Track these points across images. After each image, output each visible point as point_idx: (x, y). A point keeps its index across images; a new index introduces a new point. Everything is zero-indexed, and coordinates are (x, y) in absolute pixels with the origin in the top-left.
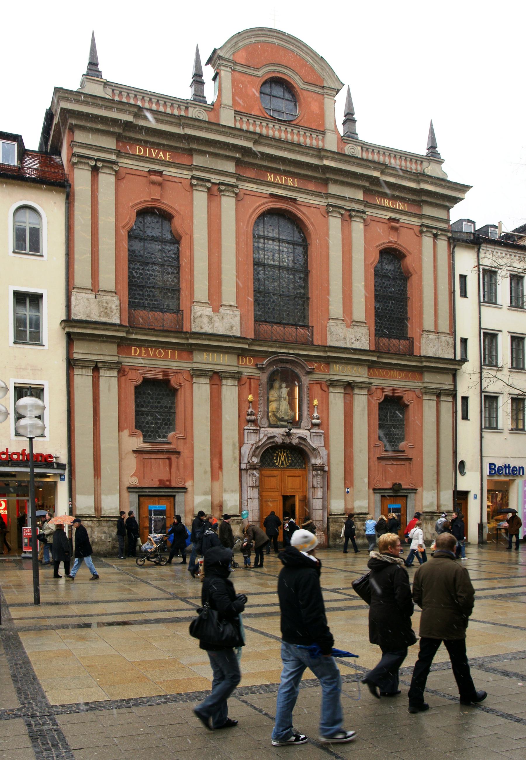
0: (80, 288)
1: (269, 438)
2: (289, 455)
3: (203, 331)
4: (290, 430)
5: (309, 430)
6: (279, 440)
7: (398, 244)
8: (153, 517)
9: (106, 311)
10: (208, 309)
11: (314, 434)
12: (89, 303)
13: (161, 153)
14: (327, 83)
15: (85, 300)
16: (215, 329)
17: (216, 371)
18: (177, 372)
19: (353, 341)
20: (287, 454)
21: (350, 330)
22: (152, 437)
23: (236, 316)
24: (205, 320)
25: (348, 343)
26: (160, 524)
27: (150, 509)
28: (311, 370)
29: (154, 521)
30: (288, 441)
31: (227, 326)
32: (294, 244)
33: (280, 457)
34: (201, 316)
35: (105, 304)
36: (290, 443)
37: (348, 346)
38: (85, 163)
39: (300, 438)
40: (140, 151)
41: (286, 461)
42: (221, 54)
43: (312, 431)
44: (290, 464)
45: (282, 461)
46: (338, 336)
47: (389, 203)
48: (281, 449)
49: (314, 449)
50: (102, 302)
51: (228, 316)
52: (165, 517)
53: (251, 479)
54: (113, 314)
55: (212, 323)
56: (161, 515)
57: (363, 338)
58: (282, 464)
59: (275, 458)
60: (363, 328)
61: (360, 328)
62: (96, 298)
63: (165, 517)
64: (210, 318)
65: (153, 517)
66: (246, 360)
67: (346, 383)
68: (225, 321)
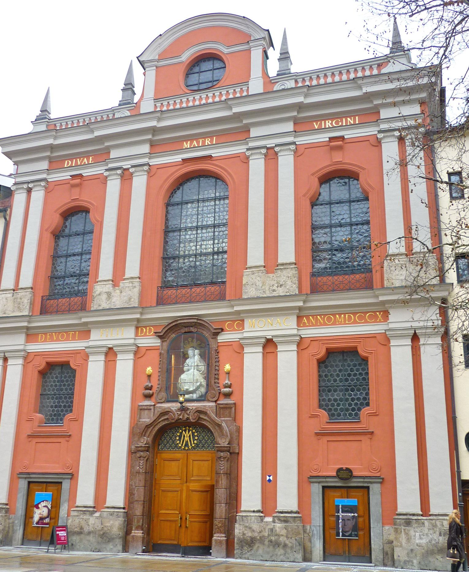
0: (4, 290)
2: (196, 434)
3: (101, 308)
6: (177, 415)
8: (341, 514)
10: (107, 286)
11: (221, 406)
12: (7, 301)
13: (85, 159)
14: (254, 37)
15: (4, 300)
18: (76, 353)
19: (275, 288)
20: (193, 433)
21: (271, 275)
22: (55, 421)
23: (135, 287)
24: (104, 297)
25: (267, 292)
26: (350, 524)
27: (336, 504)
28: (220, 331)
29: (342, 520)
31: (126, 299)
34: (99, 294)
35: (19, 300)
37: (268, 294)
41: (190, 441)
43: (218, 402)
44: (197, 445)
46: (254, 286)
47: (331, 124)
48: (189, 427)
52: (356, 515)
55: (110, 298)
56: (351, 513)
57: (289, 283)
58: (187, 445)
59: (177, 438)
60: (289, 270)
63: (356, 515)
64: (109, 294)
65: (341, 514)
67: (264, 340)
68: (124, 294)
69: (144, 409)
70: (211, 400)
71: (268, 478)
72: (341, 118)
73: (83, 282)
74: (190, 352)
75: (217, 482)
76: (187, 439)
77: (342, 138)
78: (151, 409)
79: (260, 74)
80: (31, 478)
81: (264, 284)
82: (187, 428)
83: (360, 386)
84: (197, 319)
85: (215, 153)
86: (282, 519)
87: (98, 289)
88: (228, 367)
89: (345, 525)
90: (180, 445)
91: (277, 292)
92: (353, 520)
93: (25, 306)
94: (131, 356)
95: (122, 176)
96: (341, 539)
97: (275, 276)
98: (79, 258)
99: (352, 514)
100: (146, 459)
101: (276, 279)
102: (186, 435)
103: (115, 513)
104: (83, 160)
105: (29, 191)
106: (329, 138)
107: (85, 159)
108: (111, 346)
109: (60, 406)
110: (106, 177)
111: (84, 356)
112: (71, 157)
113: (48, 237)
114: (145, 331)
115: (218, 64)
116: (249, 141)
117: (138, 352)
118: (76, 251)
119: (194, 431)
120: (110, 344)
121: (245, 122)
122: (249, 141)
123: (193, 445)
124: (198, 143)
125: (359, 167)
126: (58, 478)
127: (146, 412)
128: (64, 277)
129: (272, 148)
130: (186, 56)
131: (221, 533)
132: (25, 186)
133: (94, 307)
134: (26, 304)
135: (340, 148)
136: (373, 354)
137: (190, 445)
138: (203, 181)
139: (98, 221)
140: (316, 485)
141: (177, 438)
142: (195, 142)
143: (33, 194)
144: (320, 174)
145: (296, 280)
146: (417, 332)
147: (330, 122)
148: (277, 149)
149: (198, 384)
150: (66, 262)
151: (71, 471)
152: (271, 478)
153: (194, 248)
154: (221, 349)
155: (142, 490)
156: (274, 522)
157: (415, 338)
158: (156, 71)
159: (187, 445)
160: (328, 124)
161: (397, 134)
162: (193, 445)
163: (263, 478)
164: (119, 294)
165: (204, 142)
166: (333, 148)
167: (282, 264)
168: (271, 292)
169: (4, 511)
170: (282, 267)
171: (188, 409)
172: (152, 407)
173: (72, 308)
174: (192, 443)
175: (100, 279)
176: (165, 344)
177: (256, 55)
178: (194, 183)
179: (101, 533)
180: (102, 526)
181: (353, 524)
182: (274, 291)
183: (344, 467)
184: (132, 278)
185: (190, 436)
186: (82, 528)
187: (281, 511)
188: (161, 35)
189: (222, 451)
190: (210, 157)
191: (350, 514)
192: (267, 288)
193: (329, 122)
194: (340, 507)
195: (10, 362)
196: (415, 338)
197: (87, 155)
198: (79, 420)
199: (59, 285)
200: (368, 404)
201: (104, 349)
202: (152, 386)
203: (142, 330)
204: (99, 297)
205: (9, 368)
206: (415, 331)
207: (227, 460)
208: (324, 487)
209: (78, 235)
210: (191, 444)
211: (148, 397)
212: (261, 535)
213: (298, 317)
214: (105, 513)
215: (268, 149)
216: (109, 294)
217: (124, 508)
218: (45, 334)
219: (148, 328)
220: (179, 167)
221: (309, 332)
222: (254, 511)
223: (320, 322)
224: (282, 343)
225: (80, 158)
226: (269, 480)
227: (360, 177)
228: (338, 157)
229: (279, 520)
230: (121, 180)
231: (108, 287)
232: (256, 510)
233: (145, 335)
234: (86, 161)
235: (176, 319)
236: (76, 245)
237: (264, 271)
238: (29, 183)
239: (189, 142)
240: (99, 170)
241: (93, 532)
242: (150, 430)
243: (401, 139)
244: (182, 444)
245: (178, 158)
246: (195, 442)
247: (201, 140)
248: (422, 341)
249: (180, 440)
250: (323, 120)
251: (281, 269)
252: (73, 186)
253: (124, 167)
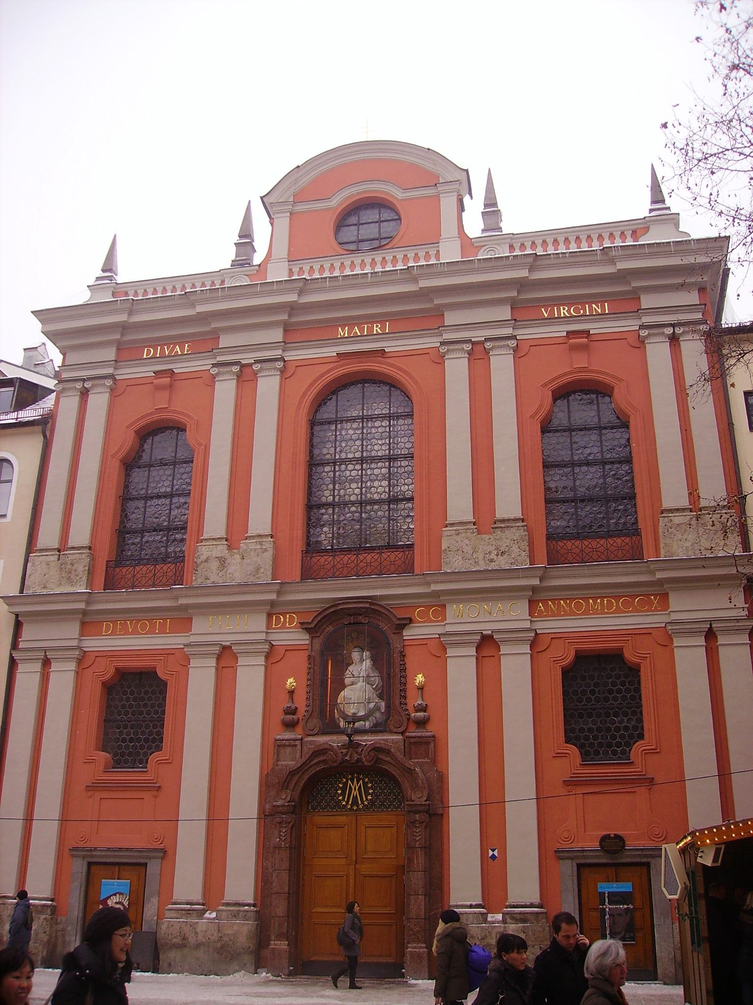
0: (43, 550)
3: (209, 583)
7: (591, 371)
9: (69, 575)
10: (220, 548)
11: (413, 740)
14: (444, 178)
15: (44, 566)
16: (228, 576)
17: (224, 644)
18: (167, 653)
19: (493, 556)
23: (266, 550)
24: (215, 565)
25: (482, 563)
32: (390, 417)
34: (206, 561)
35: (69, 567)
38: (71, 389)
40: (149, 352)
42: (271, 200)
43: (407, 734)
47: (569, 311)
48: (359, 774)
50: (66, 564)
51: (252, 553)
54: (78, 578)
57: (515, 549)
58: (355, 802)
59: (339, 792)
61: (507, 532)
62: (59, 560)
64: (222, 561)
66: (285, 618)
69: (285, 746)
70: (395, 730)
71: (491, 853)
72: (583, 304)
73: (175, 540)
74: (356, 655)
75: (410, 860)
76: (355, 792)
77: (586, 333)
78: (295, 746)
79: (455, 233)
80: (93, 856)
81: (475, 551)
83: (629, 708)
84: (371, 603)
85: (391, 346)
86: (518, 917)
87: (204, 551)
88: (420, 678)
89: (614, 923)
90: (344, 803)
91: (497, 563)
92: (627, 914)
93: (80, 576)
94: (261, 660)
95: (239, 376)
97: (492, 539)
98: (168, 501)
99: (625, 906)
100: (290, 825)
101: (494, 543)
102: (353, 788)
103: (241, 914)
104: (174, 347)
105: (84, 394)
106: (567, 332)
107: (177, 347)
108: (228, 644)
109: (139, 740)
110: (214, 377)
111: (183, 659)
112: (153, 343)
113: (115, 467)
114: (282, 620)
115: (386, 215)
116: (444, 330)
117: (271, 654)
118: (163, 490)
119: (366, 780)
120: (227, 640)
121: (437, 301)
122: (444, 330)
123: (366, 803)
124: (362, 330)
125: (614, 377)
126: (140, 857)
127: (289, 750)
128: (142, 532)
129: (482, 343)
130: (338, 201)
131: (419, 941)
132: (79, 385)
133: (198, 581)
134: (81, 573)
135: (585, 348)
136: (648, 659)
137: (360, 803)
138: (370, 388)
139: (200, 444)
140: (569, 862)
141: (339, 792)
142: (356, 328)
143: (92, 399)
144: (555, 385)
145: (525, 545)
146: (714, 626)
147: (566, 308)
148: (488, 345)
149: (372, 705)
150: (145, 507)
152: (496, 853)
153: (357, 491)
154: (408, 651)
155: (285, 876)
156: (504, 921)
157: (710, 635)
158: (290, 219)
159: (355, 802)
160: (564, 312)
161: (669, 331)
162: (366, 803)
163: (483, 853)
164: (240, 560)
165: (370, 329)
166: (574, 348)
167: (503, 521)
168: (488, 562)
169: (49, 911)
170: (503, 525)
171: (359, 745)
172: (298, 743)
173: (137, 582)
174: (364, 799)
175: (205, 536)
176: (317, 643)
177: (448, 204)
178: (354, 391)
179: (219, 945)
180: (220, 935)
181: (627, 921)
182: (492, 561)
183: (612, 833)
184: (260, 536)
185: (360, 788)
186: (184, 938)
187: (515, 904)
188: (298, 167)
189: (416, 813)
190: (382, 352)
191: (621, 906)
192: (481, 557)
193: (564, 309)
194: (606, 895)
195: (54, 666)
196: (710, 635)
197: (180, 340)
198: (175, 762)
199: (133, 544)
200: (641, 737)
201: (217, 649)
202: (296, 708)
203: (278, 619)
204: (205, 564)
205: (52, 677)
206: (711, 624)
207: (426, 827)
208: (579, 866)
209: (166, 465)
210: (362, 802)
211: (289, 725)
212: (485, 942)
213: (531, 602)
214: (224, 914)
215: (474, 344)
216: (222, 561)
217: (254, 905)
218: (115, 622)
219: (288, 616)
220: (331, 365)
221: (548, 625)
222: (471, 906)
223: (564, 610)
224: (506, 641)
225: (168, 345)
226: (493, 857)
227: (616, 391)
228: (580, 361)
229: (513, 918)
230: (238, 382)
231: (221, 549)
233: (284, 627)
234: (178, 350)
235: (336, 602)
236: (162, 481)
237: (475, 530)
238: (84, 380)
239: (347, 328)
240: (202, 364)
241: (203, 944)
242: (296, 778)
243: (674, 340)
244: (348, 801)
245: (331, 351)
246: (369, 797)
247: (366, 326)
248: (721, 640)
249: (343, 794)
250: (555, 305)
251: (501, 527)
252: (158, 388)
253: (243, 362)
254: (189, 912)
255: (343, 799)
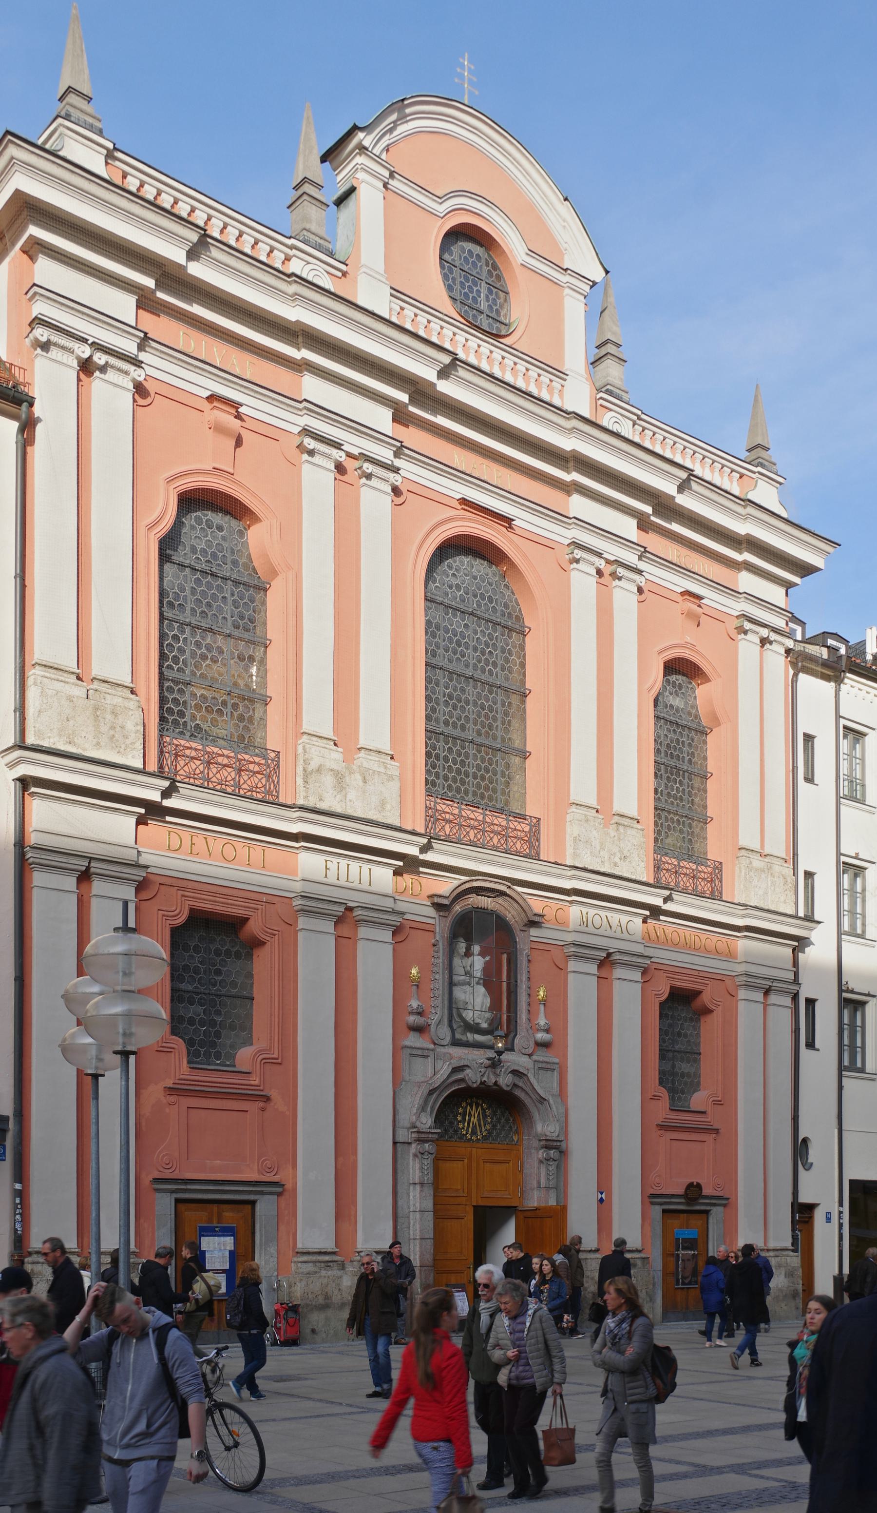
1: (456, 1070)
4: (500, 1053)
5: (530, 1055)
6: (473, 1077)
20: (484, 1110)
23: (391, 778)
30: (490, 1079)
33: (470, 1113)
36: (496, 1083)
39: (515, 1073)
41: (480, 1126)
43: (535, 1057)
44: (490, 1133)
45: (474, 1127)
49: (542, 1100)
53: (417, 1166)
58: (474, 1133)
59: (459, 1118)
64: (340, 779)
71: (600, 1196)
82: (474, 1100)
89: (685, 1268)
90: (464, 1132)
96: (681, 1288)
99: (693, 1252)
102: (473, 1114)
126: (251, 1192)
141: (459, 1118)
151: (276, 1179)
152: (603, 1196)
195: (98, 886)
205: (95, 903)
222: (590, 1251)
232: (593, 1249)
254: (329, 1264)
255: (463, 1128)
